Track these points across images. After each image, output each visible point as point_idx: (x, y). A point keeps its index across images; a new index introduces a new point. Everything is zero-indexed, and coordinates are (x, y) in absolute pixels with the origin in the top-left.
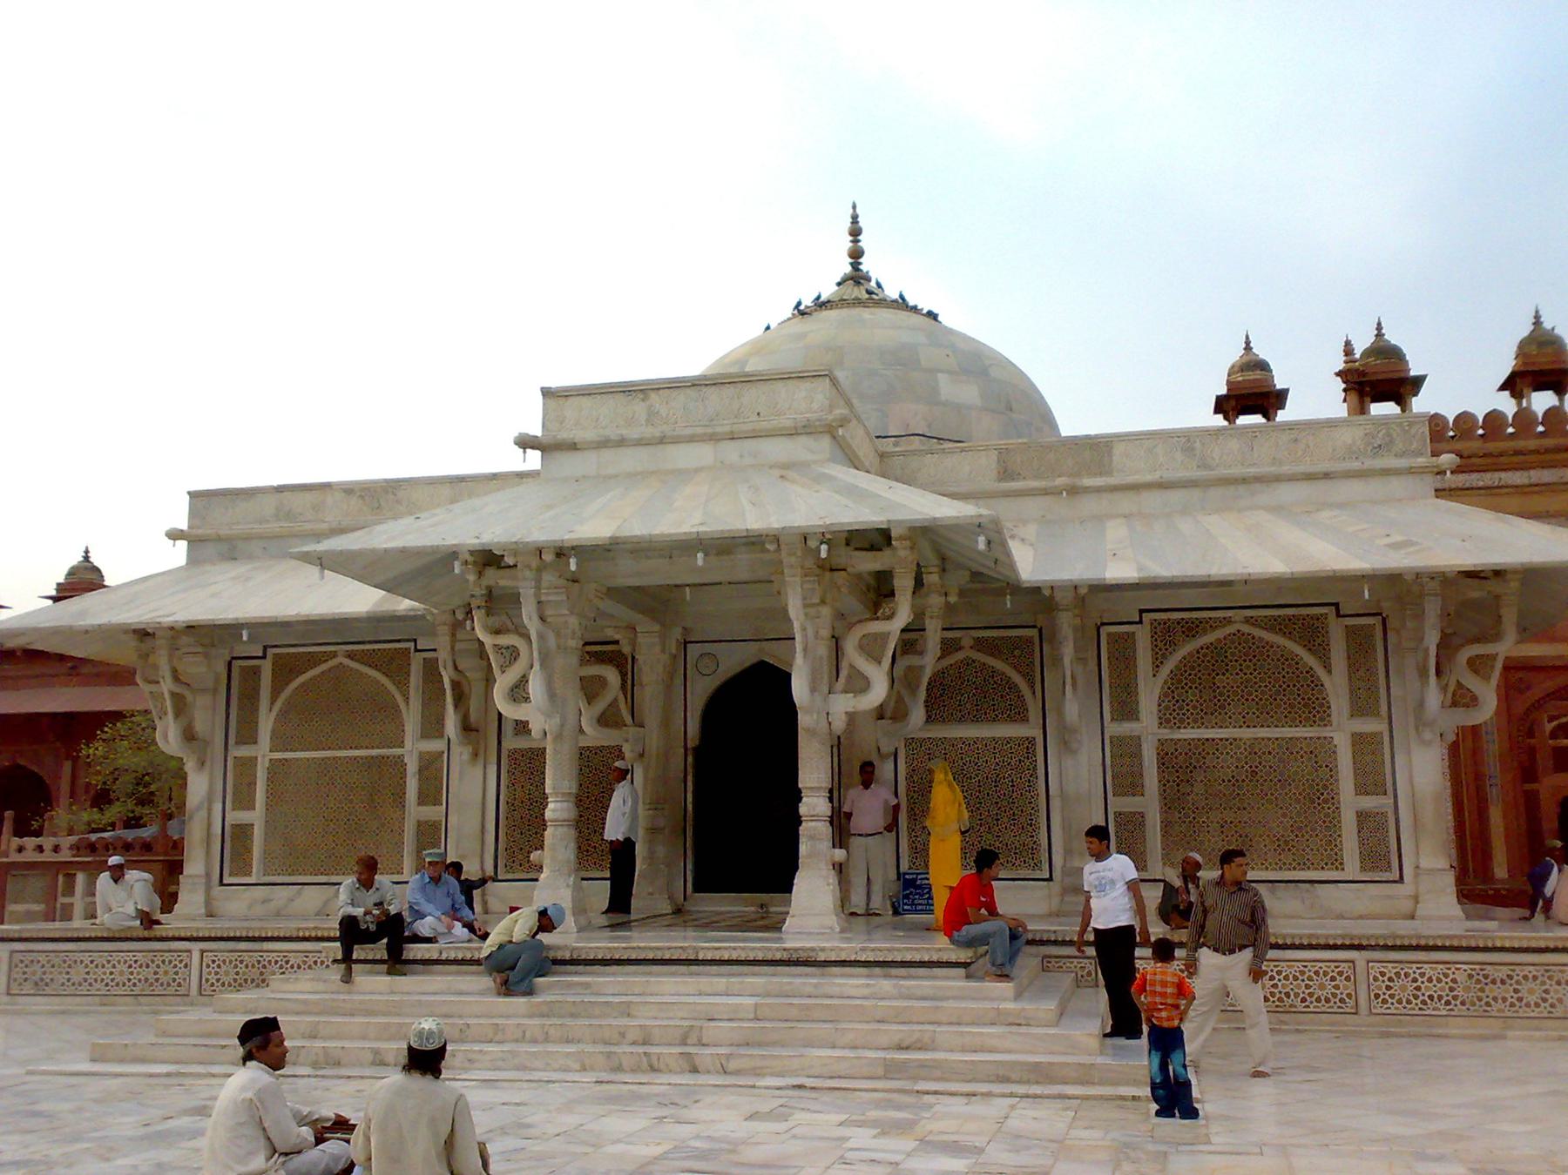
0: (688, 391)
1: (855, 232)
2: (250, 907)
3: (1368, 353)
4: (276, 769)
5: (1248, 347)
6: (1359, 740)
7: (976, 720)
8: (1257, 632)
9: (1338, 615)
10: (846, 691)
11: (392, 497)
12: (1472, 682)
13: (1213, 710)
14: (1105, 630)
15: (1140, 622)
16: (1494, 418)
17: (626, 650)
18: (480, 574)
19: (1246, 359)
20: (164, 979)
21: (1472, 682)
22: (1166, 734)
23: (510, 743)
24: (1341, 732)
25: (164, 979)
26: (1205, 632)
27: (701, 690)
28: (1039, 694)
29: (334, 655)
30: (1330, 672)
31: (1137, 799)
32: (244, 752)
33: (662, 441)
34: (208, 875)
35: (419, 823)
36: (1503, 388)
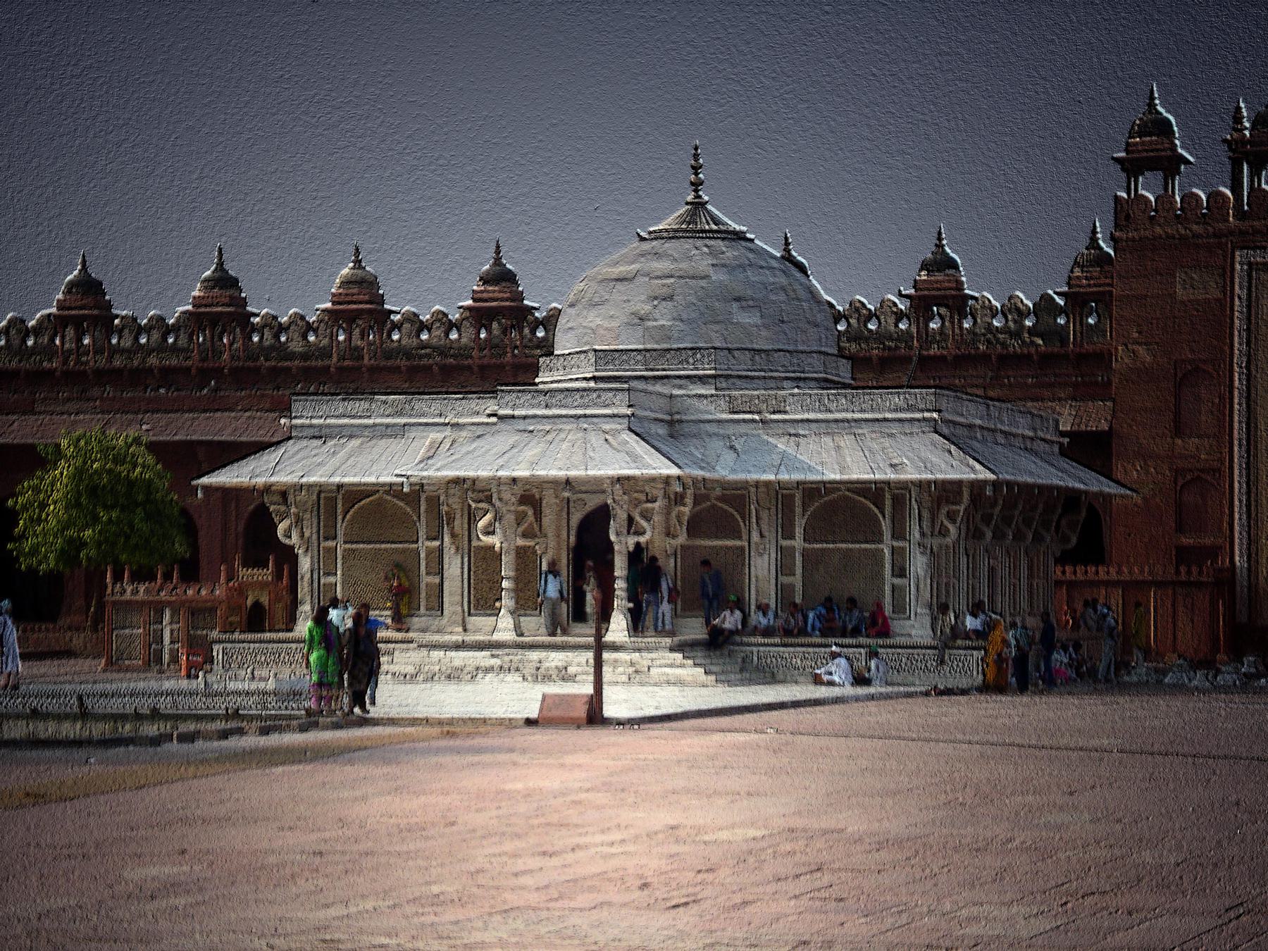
7: (717, 538)
17: (537, 496)
27: (576, 518)
30: (884, 517)
32: (331, 544)
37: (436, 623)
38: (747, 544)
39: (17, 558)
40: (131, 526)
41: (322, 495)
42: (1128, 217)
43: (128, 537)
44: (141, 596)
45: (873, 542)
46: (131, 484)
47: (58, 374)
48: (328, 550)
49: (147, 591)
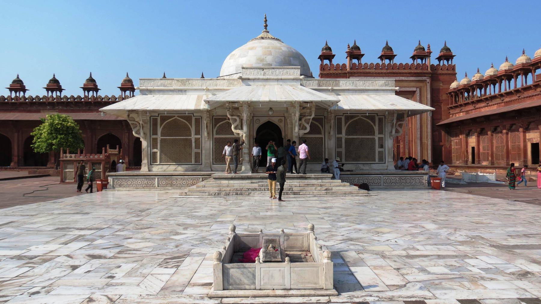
0: (273, 70)
1: (266, 21)
2: (158, 169)
3: (352, 48)
4: (162, 140)
5: (327, 44)
6: (379, 138)
8: (363, 118)
9: (377, 116)
10: (302, 129)
11: (187, 82)
12: (399, 128)
13: (355, 132)
14: (337, 117)
15: (343, 116)
16: (378, 64)
18: (229, 104)
19: (326, 47)
20: (150, 184)
21: (399, 128)
22: (347, 137)
23: (215, 136)
24: (377, 137)
25: (150, 184)
26: (354, 118)
27: (256, 126)
28: (324, 129)
29: (175, 116)
31: (341, 149)
32: (154, 137)
33: (267, 80)
34: (148, 162)
35: (195, 152)
36: (379, 58)
37: (199, 167)
38: (323, 137)
39: (34, 149)
40: (68, 140)
41: (152, 117)
42: (323, 69)
43: (67, 143)
44: (73, 158)
45: (371, 135)
46: (68, 127)
47: (47, 103)
48: (153, 139)
49: (75, 156)
